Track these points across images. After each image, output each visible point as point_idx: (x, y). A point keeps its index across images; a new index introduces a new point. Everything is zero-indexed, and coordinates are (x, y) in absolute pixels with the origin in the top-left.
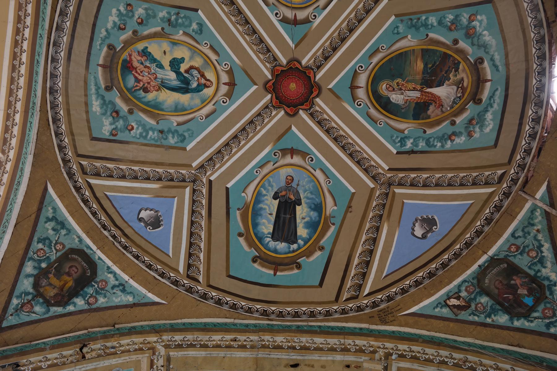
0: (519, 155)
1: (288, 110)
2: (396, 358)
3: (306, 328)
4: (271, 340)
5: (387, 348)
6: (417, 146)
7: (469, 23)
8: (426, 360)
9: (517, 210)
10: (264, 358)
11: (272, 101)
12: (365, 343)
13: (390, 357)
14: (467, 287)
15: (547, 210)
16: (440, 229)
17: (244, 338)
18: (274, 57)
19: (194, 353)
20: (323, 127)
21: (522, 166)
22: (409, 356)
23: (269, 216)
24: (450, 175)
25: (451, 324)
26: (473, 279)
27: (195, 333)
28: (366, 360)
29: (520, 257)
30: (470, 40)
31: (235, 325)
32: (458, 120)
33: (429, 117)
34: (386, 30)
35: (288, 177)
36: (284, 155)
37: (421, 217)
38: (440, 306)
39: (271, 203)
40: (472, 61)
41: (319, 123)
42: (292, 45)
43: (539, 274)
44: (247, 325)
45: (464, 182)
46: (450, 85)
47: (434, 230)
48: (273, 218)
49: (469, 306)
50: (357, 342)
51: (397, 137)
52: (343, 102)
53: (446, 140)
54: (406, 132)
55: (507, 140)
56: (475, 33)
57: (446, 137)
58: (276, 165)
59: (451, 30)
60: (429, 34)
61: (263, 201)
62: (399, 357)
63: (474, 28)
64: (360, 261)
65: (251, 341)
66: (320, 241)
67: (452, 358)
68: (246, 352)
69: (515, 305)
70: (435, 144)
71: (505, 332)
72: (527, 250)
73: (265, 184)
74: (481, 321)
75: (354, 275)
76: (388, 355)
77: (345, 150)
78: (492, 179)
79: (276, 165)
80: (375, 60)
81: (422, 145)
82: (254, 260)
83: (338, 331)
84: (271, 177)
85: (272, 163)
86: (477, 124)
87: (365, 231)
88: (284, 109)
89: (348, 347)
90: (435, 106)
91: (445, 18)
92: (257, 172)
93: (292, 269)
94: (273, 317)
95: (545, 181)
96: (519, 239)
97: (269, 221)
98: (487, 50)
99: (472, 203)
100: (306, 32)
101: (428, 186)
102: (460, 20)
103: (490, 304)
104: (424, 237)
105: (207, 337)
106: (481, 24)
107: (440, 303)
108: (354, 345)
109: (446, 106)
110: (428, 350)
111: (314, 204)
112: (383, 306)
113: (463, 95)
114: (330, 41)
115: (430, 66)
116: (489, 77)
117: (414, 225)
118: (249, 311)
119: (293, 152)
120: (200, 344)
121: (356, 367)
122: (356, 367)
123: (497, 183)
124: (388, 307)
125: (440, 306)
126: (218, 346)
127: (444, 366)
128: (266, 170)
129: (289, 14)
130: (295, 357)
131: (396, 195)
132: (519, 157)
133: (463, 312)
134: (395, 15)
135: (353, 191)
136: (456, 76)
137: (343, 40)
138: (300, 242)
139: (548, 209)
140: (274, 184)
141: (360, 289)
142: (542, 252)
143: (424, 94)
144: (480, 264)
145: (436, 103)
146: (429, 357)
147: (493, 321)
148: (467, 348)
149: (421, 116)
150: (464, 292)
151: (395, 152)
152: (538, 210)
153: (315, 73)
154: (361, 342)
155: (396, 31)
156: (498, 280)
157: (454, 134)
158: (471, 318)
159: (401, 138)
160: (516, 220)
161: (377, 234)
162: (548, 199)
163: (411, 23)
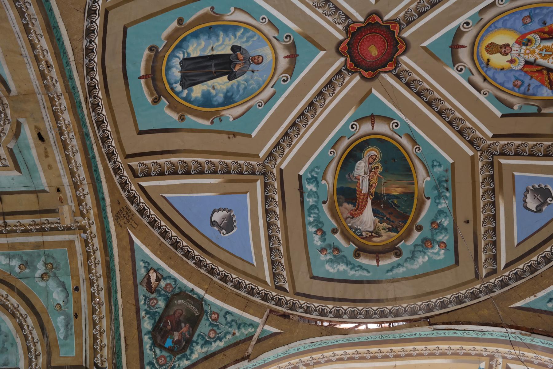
0: (304, 302)
1: (344, 44)
2: (82, 238)
3: (88, 143)
4: (63, 107)
5: (90, 227)
6: (309, 196)
7: (437, 242)
8: (89, 267)
9: (251, 311)
10: (37, 102)
11: (354, 22)
12: (90, 205)
13: (82, 231)
14: (170, 284)
15: (254, 337)
17: (55, 77)
18: (412, 21)
19: (13, 17)
20: (325, 87)
21: (293, 307)
23: (210, 48)
24: (280, 236)
25: (131, 282)
26: (179, 288)
27: (41, 16)
29: (208, 323)
30: (420, 242)
31: (68, 63)
32: (338, 236)
33: (340, 205)
34: (438, 153)
35: (261, 58)
36: (287, 47)
37: (233, 215)
38: (146, 265)
39: (227, 45)
40: (398, 245)
41: (330, 83)
42: (425, 44)
43: (194, 344)
44: (71, 78)
45: (274, 252)
46: (374, 223)
47: (222, 232)
48: (208, 53)
49: (152, 292)
51: (317, 173)
52: (356, 108)
53: (317, 225)
54: (323, 182)
55: (318, 288)
56: (427, 248)
57: (319, 225)
58: (274, 41)
59: (433, 223)
60: (430, 200)
61: (227, 36)
63: (432, 247)
64: (176, 164)
65: (54, 85)
66: (190, 114)
67: (98, 291)
68: (38, 79)
69: (162, 333)
70: (312, 215)
71: (135, 331)
72: (215, 328)
73: (248, 32)
74: (141, 307)
75: (159, 164)
76: (83, 229)
77: (300, 116)
78: (280, 279)
79: (274, 41)
80: (404, 141)
81: (310, 201)
82: (151, 49)
83: (95, 177)
84: (259, 38)
85: (276, 35)
86: (334, 256)
87: (209, 160)
88: (345, 39)
89: (80, 189)
90: (352, 210)
91: (445, 217)
92: (263, 19)
93: (151, 94)
94: (90, 99)
95: (281, 330)
96: (224, 319)
97: (204, 49)
98: (408, 260)
99: (253, 265)
100: (442, 60)
101: (267, 215)
102: (441, 233)
103: (158, 310)
104: (213, 224)
105: (40, 31)
106: (435, 254)
107: (149, 264)
108: (84, 195)
109: (352, 222)
110: (99, 267)
111: (232, 95)
112: (133, 208)
114: (429, 88)
115: (396, 202)
116: (381, 263)
117: (224, 210)
118: (89, 70)
119: (293, 57)
120: (28, 24)
123: (276, 286)
124: (133, 214)
125: (146, 265)
126: (33, 47)
127: (89, 284)
128: (267, 29)
129: (465, 40)
130: (51, 136)
131: (254, 183)
132: (302, 302)
133: (145, 289)
134: (454, 163)
135: (253, 135)
136: (384, 229)
137: (429, 104)
138: (186, 91)
139: (255, 338)
140: (250, 43)
141: (145, 176)
142: (215, 342)
143: (366, 197)
144: (195, 290)
145: (356, 210)
146: (93, 269)
147: (143, 317)
148: (112, 303)
149: (341, 196)
150: (165, 283)
151: (301, 173)
152: (253, 330)
153: (391, 72)
154: (89, 200)
155: (435, 164)
156: (182, 311)
157: (323, 233)
158: (141, 298)
159: (316, 178)
160: (242, 312)
161: (209, 173)
162: (264, 336)
163: (443, 181)
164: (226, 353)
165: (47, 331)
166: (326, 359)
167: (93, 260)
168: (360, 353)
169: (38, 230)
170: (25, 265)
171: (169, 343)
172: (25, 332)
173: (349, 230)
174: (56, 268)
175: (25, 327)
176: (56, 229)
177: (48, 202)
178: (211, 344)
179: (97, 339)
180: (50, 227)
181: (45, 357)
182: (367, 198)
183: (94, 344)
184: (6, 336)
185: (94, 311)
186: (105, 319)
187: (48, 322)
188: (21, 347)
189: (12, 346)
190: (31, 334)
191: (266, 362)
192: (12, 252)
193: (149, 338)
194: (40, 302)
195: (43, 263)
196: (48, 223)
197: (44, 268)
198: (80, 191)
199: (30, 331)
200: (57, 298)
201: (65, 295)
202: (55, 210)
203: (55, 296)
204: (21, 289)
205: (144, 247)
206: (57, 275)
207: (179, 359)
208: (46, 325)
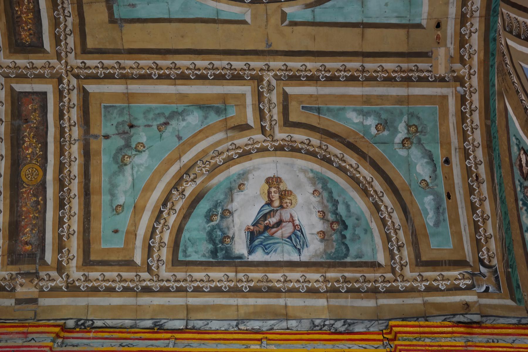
2: (459, 92)
8: (464, 132)
12: (475, 47)
13: (458, 83)
22: (465, 109)
28: (449, 50)
50: (475, 37)
62: (462, 95)
67: (476, 164)
76: (460, 80)
83: (493, 6)
89: (468, 24)
107: (519, 142)
108: (471, 32)
121: (438, 37)
122: (438, 37)
127: (462, 156)
146: (469, 136)
147: (521, 209)
148: (496, 181)
154: (475, 41)
158: (517, 183)
165: (411, 215)
167: (469, 124)
169: (403, 79)
170: (384, 125)
172: (382, 215)
174: (421, 132)
175: (383, 208)
177: (419, 40)
179: (479, 227)
180: (419, 76)
181: (411, 248)
183: (476, 233)
184: (357, 219)
185: (471, 191)
186: (487, 200)
187: (412, 204)
188: (379, 235)
189: (366, 233)
190: (391, 217)
192: (366, 107)
194: (400, 177)
195: (404, 124)
196: (417, 71)
197: (406, 131)
198: (466, 27)
199: (389, 214)
200: (422, 173)
201: (431, 169)
202: (427, 53)
203: (419, 169)
204: (376, 159)
205: (515, 119)
206: (422, 142)
208: (409, 205)
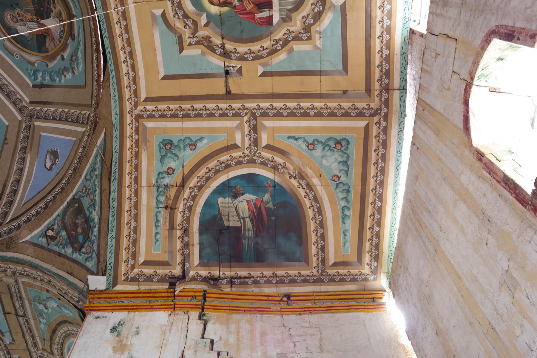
6: (44, 79)
9: (90, 153)
16: (60, 161)
29: (85, 198)
32: (66, 55)
33: (47, 51)
46: (54, 18)
54: (36, 65)
104: (51, 169)
113: (64, 29)
125: (42, 236)
133: (53, 243)
135: (7, 124)
136: (55, 8)
151: (31, 85)
159: (34, 72)
164: (103, 189)
166: (132, 83)
168: (123, 45)
169: (21, 300)
171: (81, 238)
173: (61, 44)
176: (18, 288)
178: (95, 200)
182: (40, 24)
191: (118, 151)
193: (76, 253)
207: (92, 235)
